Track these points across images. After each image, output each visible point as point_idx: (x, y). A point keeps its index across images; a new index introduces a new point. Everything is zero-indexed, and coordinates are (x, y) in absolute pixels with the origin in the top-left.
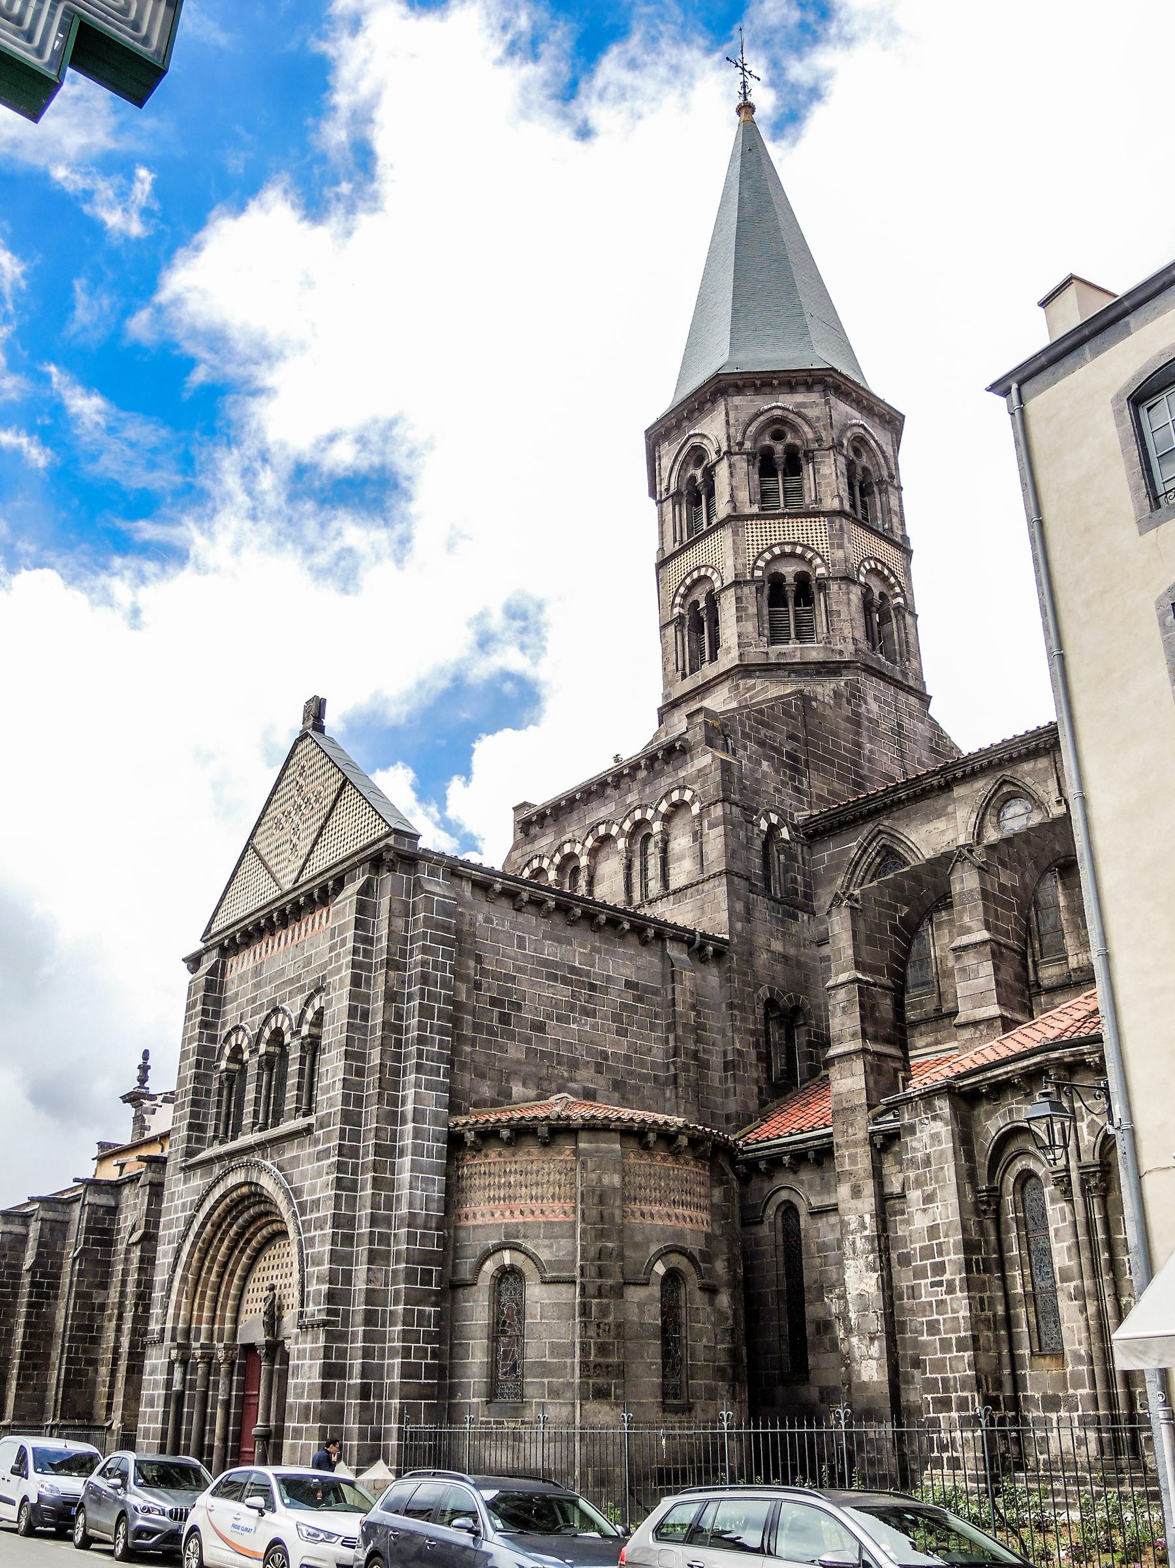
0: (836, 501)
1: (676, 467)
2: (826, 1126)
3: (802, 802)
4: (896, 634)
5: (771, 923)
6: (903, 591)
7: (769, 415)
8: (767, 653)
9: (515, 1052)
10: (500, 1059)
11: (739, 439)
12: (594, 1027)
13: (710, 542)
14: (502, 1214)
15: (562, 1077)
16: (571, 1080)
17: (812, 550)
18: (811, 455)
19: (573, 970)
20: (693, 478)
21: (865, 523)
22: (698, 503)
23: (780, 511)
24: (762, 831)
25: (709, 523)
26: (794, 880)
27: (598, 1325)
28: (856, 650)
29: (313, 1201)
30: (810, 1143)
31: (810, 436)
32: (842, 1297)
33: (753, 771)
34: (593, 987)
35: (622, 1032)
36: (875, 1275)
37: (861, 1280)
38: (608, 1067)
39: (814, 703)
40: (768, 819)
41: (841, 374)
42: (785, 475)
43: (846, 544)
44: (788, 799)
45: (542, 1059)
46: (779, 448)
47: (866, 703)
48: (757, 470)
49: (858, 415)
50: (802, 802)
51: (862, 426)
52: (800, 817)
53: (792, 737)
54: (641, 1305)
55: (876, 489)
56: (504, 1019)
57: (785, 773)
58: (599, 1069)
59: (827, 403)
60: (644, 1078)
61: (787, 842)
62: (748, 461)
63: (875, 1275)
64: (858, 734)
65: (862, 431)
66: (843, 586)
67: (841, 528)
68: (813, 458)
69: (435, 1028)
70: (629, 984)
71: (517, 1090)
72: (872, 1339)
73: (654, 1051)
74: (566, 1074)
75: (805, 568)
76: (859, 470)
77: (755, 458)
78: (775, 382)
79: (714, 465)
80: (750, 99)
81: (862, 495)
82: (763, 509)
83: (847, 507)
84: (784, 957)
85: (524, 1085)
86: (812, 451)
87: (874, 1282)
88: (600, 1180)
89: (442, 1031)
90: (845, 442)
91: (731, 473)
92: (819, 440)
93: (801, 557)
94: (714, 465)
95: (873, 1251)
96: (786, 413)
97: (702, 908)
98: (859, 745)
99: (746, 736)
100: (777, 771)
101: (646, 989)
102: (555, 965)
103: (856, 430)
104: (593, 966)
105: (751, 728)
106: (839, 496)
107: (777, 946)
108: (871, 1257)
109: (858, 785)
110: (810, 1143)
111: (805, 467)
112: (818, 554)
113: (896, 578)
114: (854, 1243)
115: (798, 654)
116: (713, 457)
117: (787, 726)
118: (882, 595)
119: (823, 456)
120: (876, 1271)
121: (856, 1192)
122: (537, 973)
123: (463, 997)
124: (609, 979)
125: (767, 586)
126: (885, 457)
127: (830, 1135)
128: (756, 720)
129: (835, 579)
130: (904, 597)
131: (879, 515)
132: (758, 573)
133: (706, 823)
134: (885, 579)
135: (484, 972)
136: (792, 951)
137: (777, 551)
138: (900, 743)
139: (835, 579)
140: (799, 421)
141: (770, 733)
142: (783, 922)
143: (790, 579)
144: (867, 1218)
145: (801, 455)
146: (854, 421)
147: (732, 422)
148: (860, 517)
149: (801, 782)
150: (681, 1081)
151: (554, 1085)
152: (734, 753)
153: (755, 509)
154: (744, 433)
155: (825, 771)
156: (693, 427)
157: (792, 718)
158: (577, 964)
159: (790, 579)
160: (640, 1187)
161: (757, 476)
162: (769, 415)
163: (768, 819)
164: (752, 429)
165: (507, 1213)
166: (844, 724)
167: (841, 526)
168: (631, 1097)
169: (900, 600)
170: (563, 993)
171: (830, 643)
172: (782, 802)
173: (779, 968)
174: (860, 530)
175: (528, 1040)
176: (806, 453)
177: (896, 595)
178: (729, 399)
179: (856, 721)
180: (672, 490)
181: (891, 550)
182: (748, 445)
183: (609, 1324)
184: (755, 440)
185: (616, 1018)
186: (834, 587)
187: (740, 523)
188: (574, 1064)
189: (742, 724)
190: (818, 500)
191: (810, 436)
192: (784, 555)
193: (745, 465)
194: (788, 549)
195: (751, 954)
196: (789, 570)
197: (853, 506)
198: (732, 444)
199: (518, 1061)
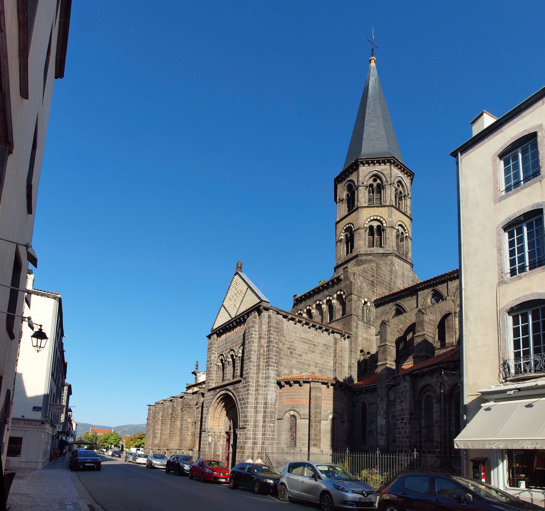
2: (375, 383)
3: (374, 295)
4: (405, 245)
5: (363, 329)
6: (408, 232)
8: (367, 251)
9: (294, 361)
10: (290, 364)
12: (315, 356)
14: (291, 402)
15: (306, 369)
16: (309, 369)
17: (383, 218)
18: (384, 187)
19: (309, 340)
21: (398, 210)
23: (374, 205)
24: (362, 303)
26: (370, 317)
27: (315, 429)
28: (393, 250)
29: (242, 398)
30: (370, 387)
32: (376, 425)
33: (361, 286)
34: (315, 345)
35: (322, 357)
36: (385, 420)
37: (381, 421)
38: (318, 366)
39: (380, 266)
40: (364, 300)
43: (393, 216)
44: (370, 294)
45: (301, 364)
46: (375, 184)
47: (394, 266)
50: (374, 295)
51: (401, 177)
52: (373, 300)
53: (373, 276)
54: (325, 425)
55: (403, 198)
56: (291, 353)
57: (370, 286)
58: (316, 367)
60: (328, 369)
61: (369, 307)
63: (385, 420)
64: (391, 275)
65: (401, 178)
66: (391, 230)
67: (392, 211)
69: (274, 355)
70: (324, 345)
71: (295, 371)
72: (383, 435)
73: (330, 363)
74: (307, 368)
75: (380, 224)
76: (399, 192)
77: (367, 188)
81: (399, 200)
83: (394, 204)
84: (366, 338)
85: (296, 370)
86: (385, 185)
87: (385, 422)
88: (316, 395)
89: (276, 356)
90: (395, 182)
93: (379, 221)
95: (385, 414)
97: (344, 325)
98: (391, 279)
99: (359, 275)
100: (368, 286)
101: (329, 346)
102: (305, 339)
103: (399, 178)
104: (315, 339)
105: (361, 273)
107: (365, 336)
108: (385, 416)
109: (390, 290)
110: (370, 387)
111: (382, 191)
112: (384, 219)
113: (407, 227)
114: (380, 412)
115: (376, 251)
117: (371, 272)
118: (402, 233)
119: (388, 187)
120: (385, 419)
121: (382, 400)
122: (300, 341)
123: (281, 347)
124: (319, 343)
125: (368, 229)
127: (376, 385)
128: (363, 271)
129: (389, 227)
130: (409, 234)
132: (366, 225)
133: (347, 301)
134: (403, 228)
135: (286, 340)
136: (368, 337)
137: (372, 218)
138: (403, 279)
139: (389, 227)
141: (366, 274)
142: (366, 329)
143: (375, 227)
144: (384, 406)
146: (399, 175)
148: (397, 207)
149: (374, 289)
150: (337, 370)
151: (304, 370)
152: (356, 280)
153: (366, 205)
154: (365, 179)
155: (381, 286)
157: (373, 270)
158: (310, 339)
159: (375, 227)
160: (326, 397)
163: (364, 300)
165: (292, 402)
166: (388, 272)
168: (324, 374)
169: (407, 234)
170: (306, 346)
171: (385, 247)
172: (368, 295)
173: (365, 341)
174: (397, 212)
175: (297, 359)
177: (406, 233)
179: (391, 271)
181: (406, 218)
183: (317, 429)
185: (321, 354)
186: (388, 230)
187: (361, 209)
188: (309, 365)
189: (359, 271)
190: (385, 202)
192: (374, 220)
193: (364, 190)
194: (375, 218)
195: (357, 337)
196: (375, 224)
197: (396, 204)
199: (295, 364)
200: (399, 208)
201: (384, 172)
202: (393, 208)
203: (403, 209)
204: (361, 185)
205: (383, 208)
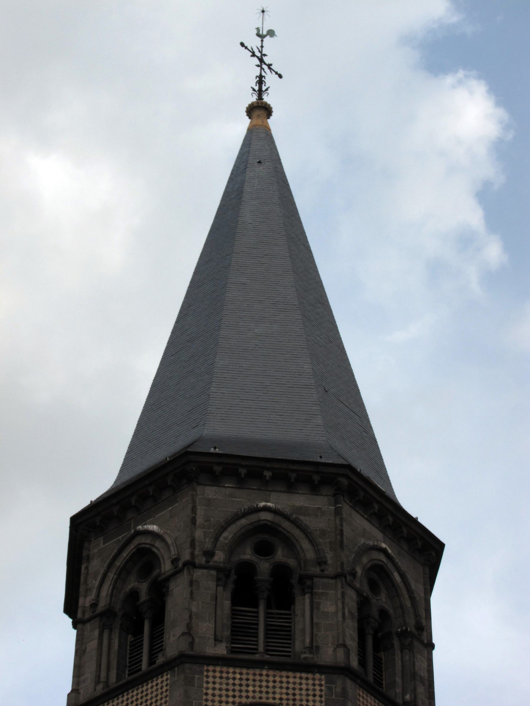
0: (341, 653)
1: (111, 575)
7: (253, 518)
11: (208, 546)
13: (150, 688)
18: (309, 583)
20: (134, 594)
22: (138, 631)
23: (257, 657)
25: (151, 662)
31: (310, 555)
41: (359, 475)
42: (268, 606)
48: (228, 594)
49: (379, 535)
55: (396, 642)
59: (338, 512)
62: (218, 579)
67: (344, 690)
68: (311, 588)
76: (375, 613)
77: (228, 576)
78: (268, 474)
79: (168, 579)
80: (266, 99)
81: (376, 649)
82: (233, 651)
83: (354, 663)
86: (311, 577)
90: (359, 571)
91: (192, 593)
92: (321, 562)
94: (168, 579)
96: (278, 519)
106: (344, 646)
111: (298, 599)
116: (167, 567)
126: (412, 599)
131: (398, 680)
140: (296, 532)
145: (294, 581)
147: (199, 520)
153: (221, 650)
154: (217, 538)
156: (143, 521)
161: (227, 604)
162: (253, 518)
164: (228, 535)
167: (344, 690)
176: (302, 579)
178: (199, 489)
180: (103, 604)
182: (219, 557)
184: (232, 550)
190: (313, 648)
191: (310, 555)
193: (212, 584)
197: (362, 662)
198: (197, 552)
200: (378, 681)
201: (306, 520)
202: (349, 683)
203: (399, 690)
204: (201, 560)
205: (304, 675)
